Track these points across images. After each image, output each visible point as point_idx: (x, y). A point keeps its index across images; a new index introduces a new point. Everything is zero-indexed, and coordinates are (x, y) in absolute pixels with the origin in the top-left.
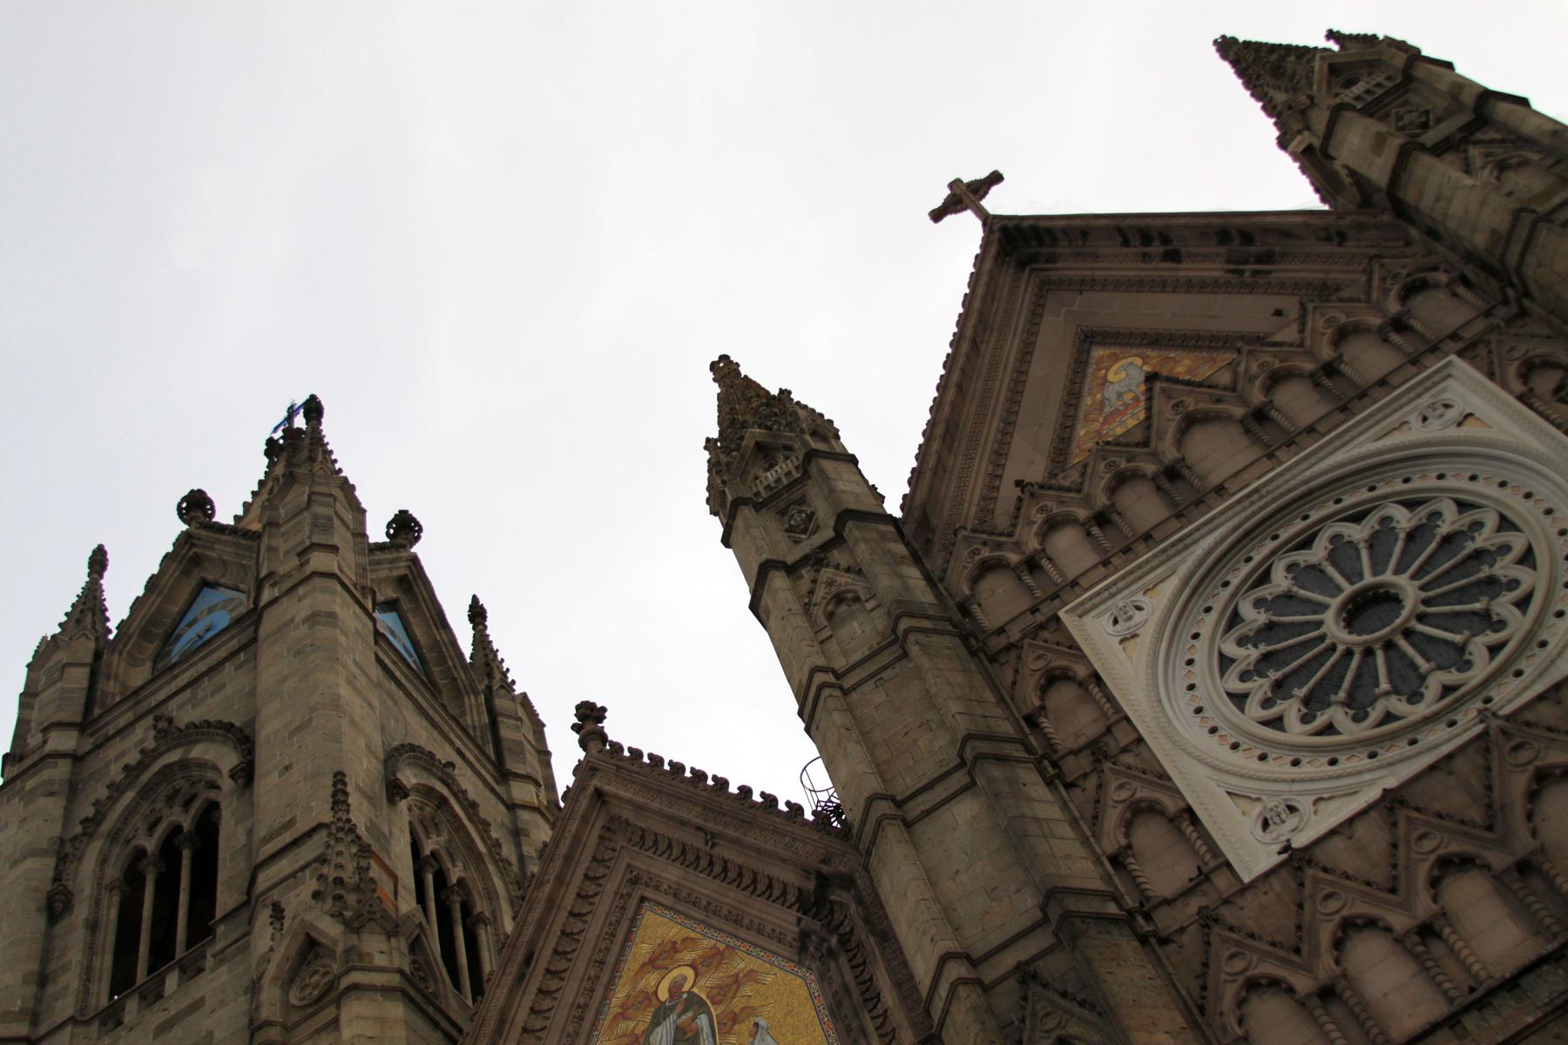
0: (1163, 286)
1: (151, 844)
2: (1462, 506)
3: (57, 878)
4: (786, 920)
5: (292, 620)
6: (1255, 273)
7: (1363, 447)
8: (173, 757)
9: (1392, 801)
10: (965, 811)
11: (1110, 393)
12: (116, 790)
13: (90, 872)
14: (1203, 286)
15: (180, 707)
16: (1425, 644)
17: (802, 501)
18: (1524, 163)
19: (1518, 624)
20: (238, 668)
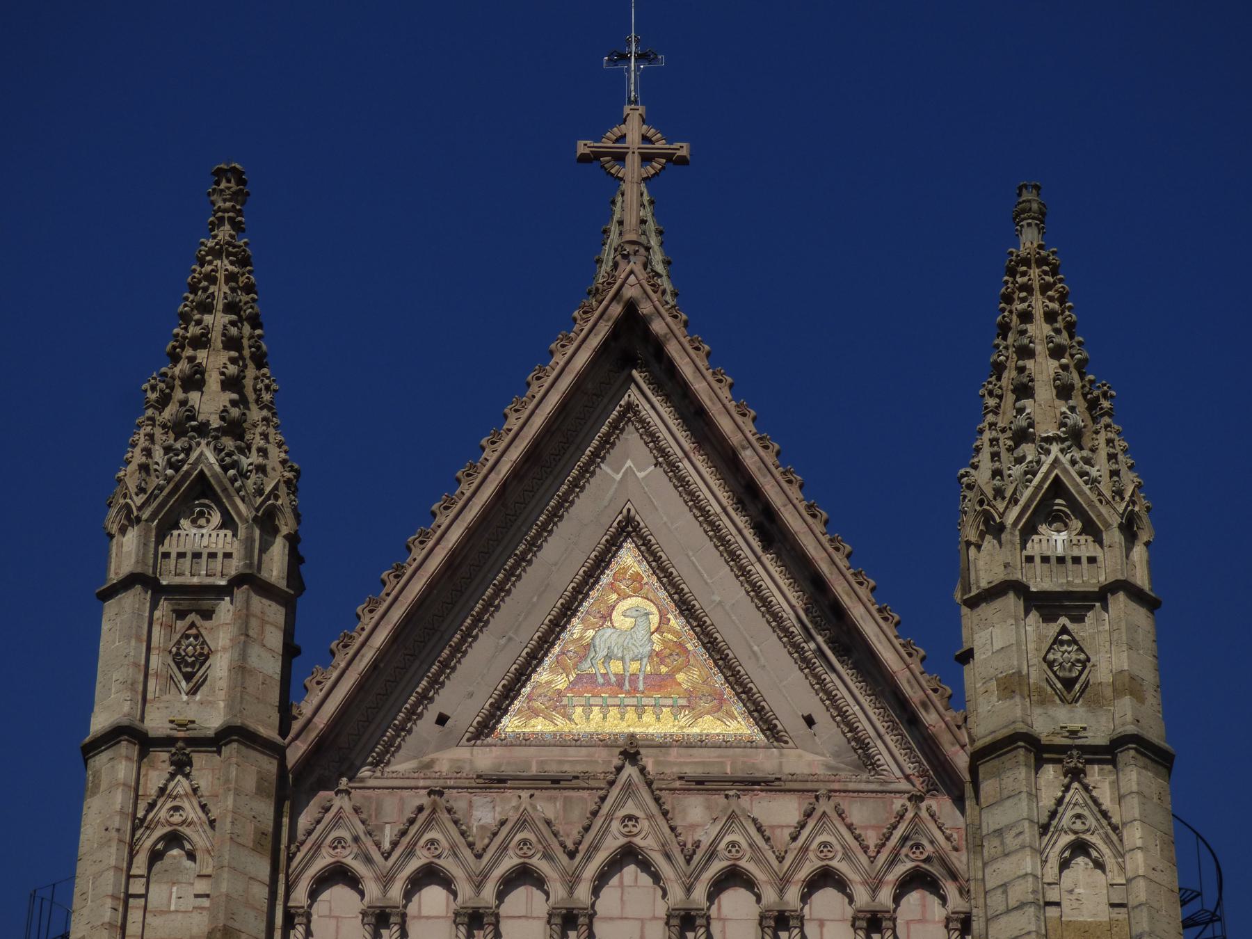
0: (733, 557)
6: (820, 652)
11: (606, 639)
14: (765, 604)
17: (207, 615)
18: (1099, 865)
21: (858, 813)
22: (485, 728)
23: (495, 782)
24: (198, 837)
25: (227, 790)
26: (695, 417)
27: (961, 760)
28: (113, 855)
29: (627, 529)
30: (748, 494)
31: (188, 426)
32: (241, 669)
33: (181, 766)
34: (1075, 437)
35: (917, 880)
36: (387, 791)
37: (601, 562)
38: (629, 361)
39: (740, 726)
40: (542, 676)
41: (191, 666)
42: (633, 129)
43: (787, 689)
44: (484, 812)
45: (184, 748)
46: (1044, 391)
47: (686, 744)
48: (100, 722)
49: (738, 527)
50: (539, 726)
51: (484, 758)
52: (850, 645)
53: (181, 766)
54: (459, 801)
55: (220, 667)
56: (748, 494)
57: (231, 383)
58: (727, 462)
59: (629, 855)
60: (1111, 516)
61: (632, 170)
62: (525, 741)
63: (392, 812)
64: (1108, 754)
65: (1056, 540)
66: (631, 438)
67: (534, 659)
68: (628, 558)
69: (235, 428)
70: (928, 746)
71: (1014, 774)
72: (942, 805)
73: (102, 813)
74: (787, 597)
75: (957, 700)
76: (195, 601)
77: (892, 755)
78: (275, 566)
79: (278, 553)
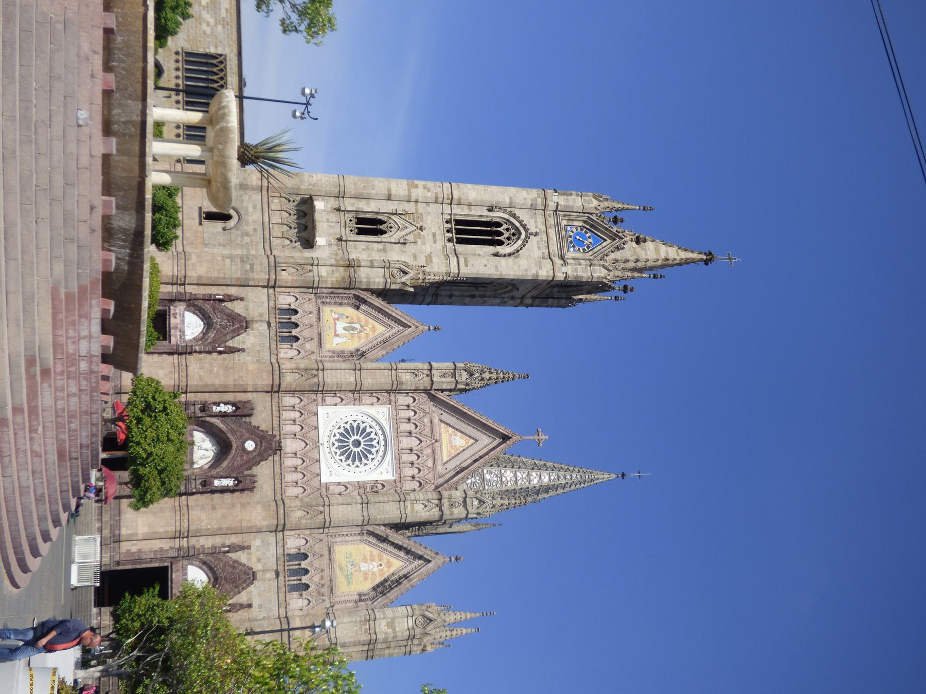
1: (500, 229)
2: (366, 464)
3: (500, 208)
4: (363, 349)
5: (541, 269)
7: (389, 457)
8: (523, 236)
9: (317, 428)
10: (352, 379)
11: (458, 438)
12: (521, 222)
13: (497, 215)
15: (541, 238)
16: (345, 446)
19: (337, 457)
20: (543, 253)
21: (430, 476)
22: (441, 421)
23: (431, 422)
24: (417, 379)
25: (424, 382)
26: (494, 449)
27: (440, 489)
28: (413, 367)
29: (476, 441)
30: (481, 457)
31: (482, 372)
32: (443, 382)
33: (427, 375)
34: (494, 506)
35: (421, 484)
36: (429, 406)
37: (470, 437)
38: (503, 438)
39: (445, 459)
40: (451, 429)
41: (444, 376)
42: (544, 437)
43: (451, 466)
44: (426, 420)
45: (430, 376)
46: (502, 502)
47: (441, 451)
48: (433, 364)
49: (477, 456)
50: (443, 429)
51: (436, 421)
52: (458, 473)
53: (427, 375)
54: (428, 416)
55: (444, 380)
56: (481, 457)
57: (490, 378)
58: (487, 454)
59: (421, 441)
60: (480, 511)
61: (536, 437)
62: (440, 427)
63: (426, 407)
64: (441, 510)
65: (476, 503)
66: (491, 440)
67: (453, 428)
68: (472, 441)
69: (482, 379)
70: (442, 485)
71: (436, 496)
72: (433, 487)
73: (419, 365)
74: (465, 464)
75: (450, 489)
76: (454, 375)
77: (441, 480)
78: (460, 386)
79: (463, 387)
